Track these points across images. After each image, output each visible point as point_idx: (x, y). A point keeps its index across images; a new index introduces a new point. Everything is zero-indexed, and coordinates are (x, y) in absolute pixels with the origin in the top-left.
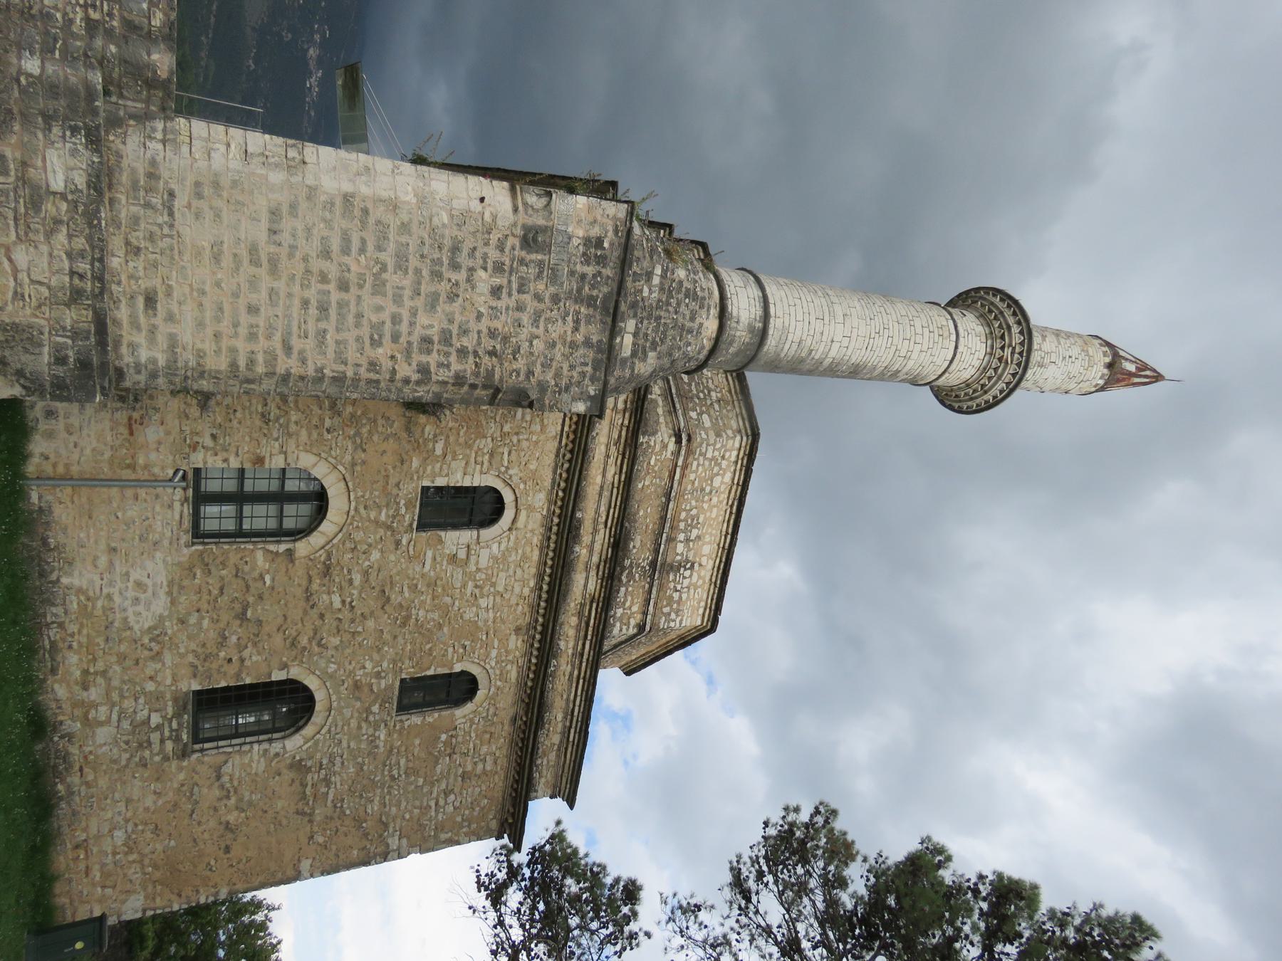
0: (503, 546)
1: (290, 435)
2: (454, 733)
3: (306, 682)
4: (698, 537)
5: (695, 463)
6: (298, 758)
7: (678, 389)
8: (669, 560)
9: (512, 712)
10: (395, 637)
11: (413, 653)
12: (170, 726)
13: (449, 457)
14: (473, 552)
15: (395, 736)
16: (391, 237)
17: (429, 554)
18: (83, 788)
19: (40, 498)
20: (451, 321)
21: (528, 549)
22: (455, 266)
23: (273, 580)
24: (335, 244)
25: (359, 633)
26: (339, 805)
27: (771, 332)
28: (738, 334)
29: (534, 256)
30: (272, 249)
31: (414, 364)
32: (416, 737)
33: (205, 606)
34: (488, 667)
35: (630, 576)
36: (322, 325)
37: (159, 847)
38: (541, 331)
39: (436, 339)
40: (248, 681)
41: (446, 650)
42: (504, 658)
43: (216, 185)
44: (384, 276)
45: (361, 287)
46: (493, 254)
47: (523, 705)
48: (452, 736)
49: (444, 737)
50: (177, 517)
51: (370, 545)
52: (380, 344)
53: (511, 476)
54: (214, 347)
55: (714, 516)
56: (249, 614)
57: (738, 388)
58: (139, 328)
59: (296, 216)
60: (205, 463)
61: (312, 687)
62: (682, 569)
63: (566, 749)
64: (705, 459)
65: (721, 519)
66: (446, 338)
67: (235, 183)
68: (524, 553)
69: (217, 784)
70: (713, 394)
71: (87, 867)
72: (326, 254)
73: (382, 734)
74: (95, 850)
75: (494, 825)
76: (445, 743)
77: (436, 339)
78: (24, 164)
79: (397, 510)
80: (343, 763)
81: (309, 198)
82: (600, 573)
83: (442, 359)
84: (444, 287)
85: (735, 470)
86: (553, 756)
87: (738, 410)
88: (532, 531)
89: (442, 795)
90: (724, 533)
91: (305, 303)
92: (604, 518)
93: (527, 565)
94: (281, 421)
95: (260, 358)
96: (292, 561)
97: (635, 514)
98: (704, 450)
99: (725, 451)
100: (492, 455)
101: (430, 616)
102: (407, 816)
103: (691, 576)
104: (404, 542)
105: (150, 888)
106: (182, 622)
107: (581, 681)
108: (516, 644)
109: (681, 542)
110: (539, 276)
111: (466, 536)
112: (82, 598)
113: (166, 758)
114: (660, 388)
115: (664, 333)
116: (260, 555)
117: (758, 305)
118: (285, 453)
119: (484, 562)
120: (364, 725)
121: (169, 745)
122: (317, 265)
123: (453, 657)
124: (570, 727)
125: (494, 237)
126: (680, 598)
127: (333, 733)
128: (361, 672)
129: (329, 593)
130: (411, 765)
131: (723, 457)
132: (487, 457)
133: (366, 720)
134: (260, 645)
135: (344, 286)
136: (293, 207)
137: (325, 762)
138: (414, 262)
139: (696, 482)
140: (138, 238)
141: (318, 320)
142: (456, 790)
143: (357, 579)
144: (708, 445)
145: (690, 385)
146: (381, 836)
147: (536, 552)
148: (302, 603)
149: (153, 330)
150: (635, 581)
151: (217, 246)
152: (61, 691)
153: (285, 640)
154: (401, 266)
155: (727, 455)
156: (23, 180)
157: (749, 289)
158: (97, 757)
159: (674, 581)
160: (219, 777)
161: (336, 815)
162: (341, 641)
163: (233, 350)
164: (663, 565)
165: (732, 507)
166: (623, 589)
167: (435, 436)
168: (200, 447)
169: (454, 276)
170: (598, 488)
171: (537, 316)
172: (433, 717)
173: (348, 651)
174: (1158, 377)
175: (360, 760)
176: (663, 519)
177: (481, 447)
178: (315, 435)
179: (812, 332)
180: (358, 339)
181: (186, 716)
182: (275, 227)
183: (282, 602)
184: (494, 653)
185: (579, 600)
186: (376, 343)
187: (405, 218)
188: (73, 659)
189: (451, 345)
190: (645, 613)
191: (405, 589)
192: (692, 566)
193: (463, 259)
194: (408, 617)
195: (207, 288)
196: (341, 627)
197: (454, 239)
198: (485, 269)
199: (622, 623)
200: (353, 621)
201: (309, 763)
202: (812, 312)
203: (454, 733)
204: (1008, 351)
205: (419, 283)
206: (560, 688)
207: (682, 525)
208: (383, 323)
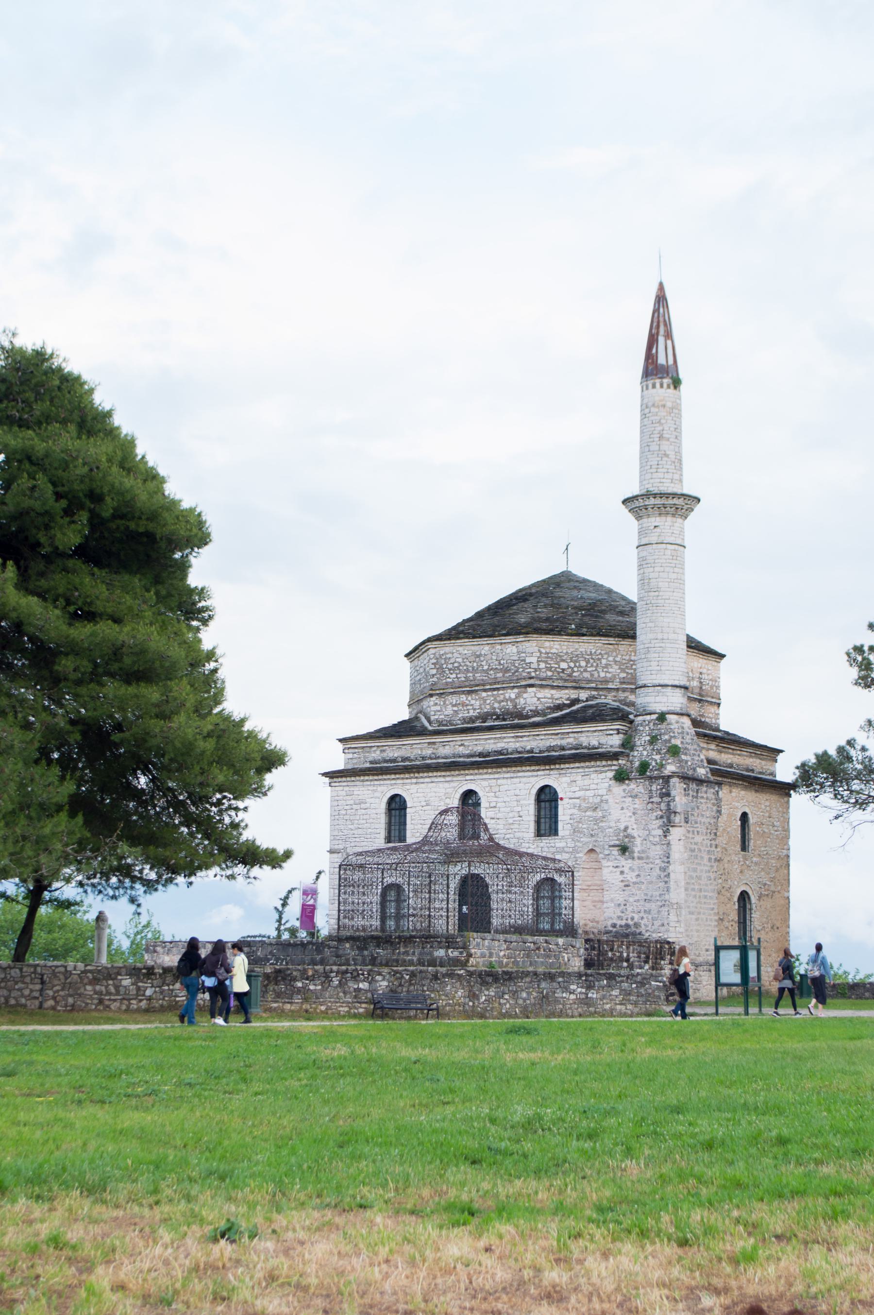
9: (753, 793)
24: (693, 893)
35: (702, 716)
73: (754, 859)
75: (786, 799)
86: (763, 763)
136: (689, 907)
140: (697, 953)
145: (627, 673)
151: (698, 931)
164: (700, 695)
171: (703, 815)
174: (661, 287)
184: (737, 804)
193: (693, 846)
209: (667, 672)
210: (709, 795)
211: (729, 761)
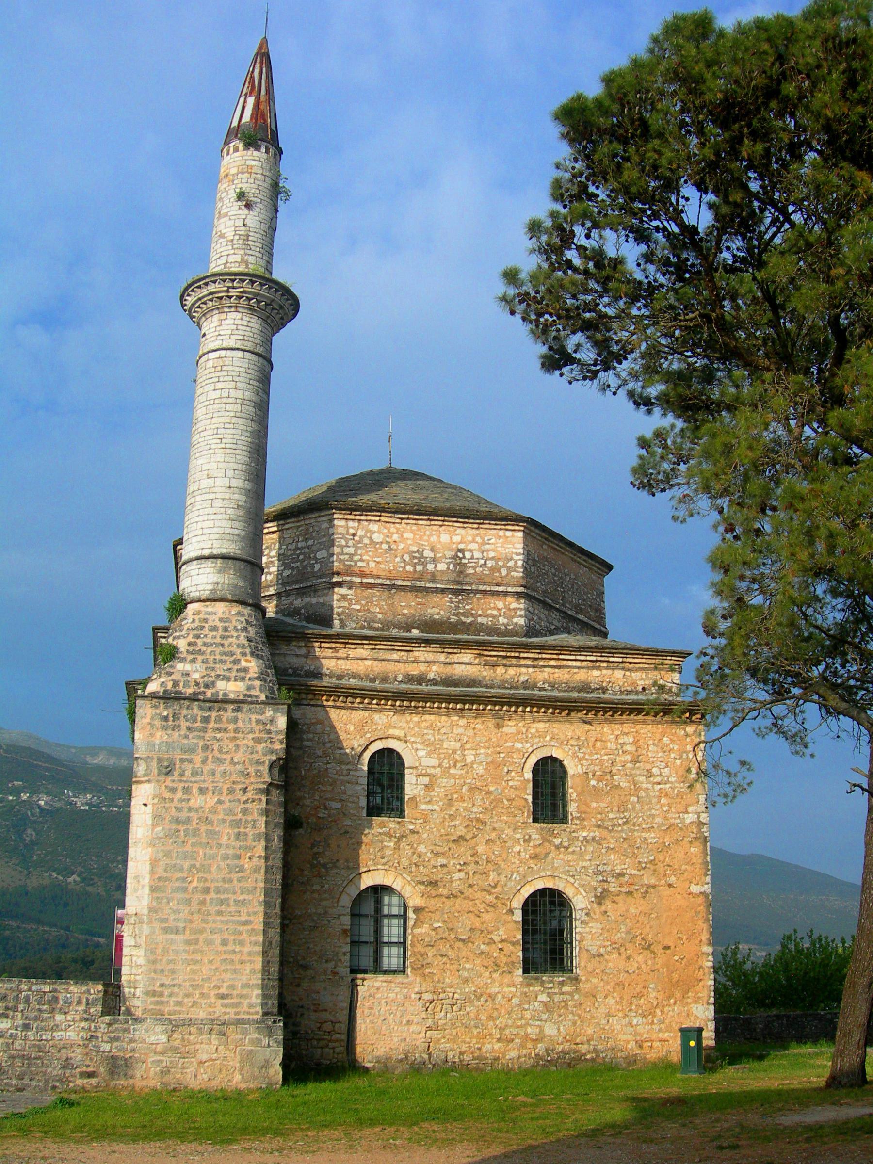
0: (419, 746)
1: (326, 913)
2: (590, 774)
3: (527, 895)
4: (432, 550)
5: (360, 564)
6: (593, 899)
7: (297, 582)
8: (453, 576)
10: (494, 829)
11: (509, 814)
12: (551, 988)
13: (344, 797)
14: (424, 771)
15: (586, 823)
16: (174, 862)
17: (423, 807)
18: (592, 1043)
19: (370, 1062)
20: (224, 821)
21: (424, 724)
22: (188, 820)
23: (438, 921)
24: (180, 895)
25: (488, 857)
26: (643, 865)
27: (224, 551)
28: (227, 582)
29: (177, 766)
30: (187, 932)
31: (254, 844)
32: (589, 807)
33: (455, 966)
34: (530, 750)
36: (232, 903)
37: (653, 994)
38: (228, 757)
39: (236, 830)
40: (519, 936)
41: (511, 787)
42: (524, 736)
43: (154, 962)
44: (198, 866)
45: (206, 880)
46: (179, 795)
47: (573, 714)
48: (593, 775)
49: (593, 782)
50: (384, 984)
51: (414, 853)
52: (243, 866)
53: (359, 746)
54: (248, 964)
55: (411, 536)
56: (463, 937)
57: (293, 520)
58: (240, 1003)
59: (167, 919)
60: (346, 967)
61: (531, 891)
62: (464, 561)
63: (630, 663)
64: (356, 554)
65: (414, 528)
66: (237, 823)
67: (153, 952)
68: (427, 728)
69: (606, 957)
70: (300, 545)
71: (660, 1041)
72: (188, 902)
74: (645, 1036)
76: (599, 781)
77: (236, 830)
78: (155, 1053)
79: (385, 834)
80: (605, 864)
81: (156, 912)
82: (455, 651)
83: (250, 825)
84: (203, 828)
85: (367, 521)
86: (636, 675)
87: (312, 521)
88: (407, 722)
89: (652, 779)
90: (428, 523)
91: (220, 913)
92: (403, 653)
93: (439, 724)
94: (315, 918)
95: (253, 939)
96: (423, 909)
97: (408, 618)
98: (347, 557)
99: (348, 533)
100: (341, 763)
101: (478, 802)
102: (665, 808)
103: (471, 551)
104: (412, 827)
105: (689, 1000)
106: (466, 981)
107: (561, 657)
108: (511, 727)
109: (436, 566)
110: (190, 761)
111: (409, 778)
112: (443, 1041)
113: (577, 990)
114: (296, 599)
115: (225, 654)
116: (417, 931)
117: (203, 566)
118: (339, 916)
119: (434, 762)
120: (570, 850)
121: (566, 989)
122: (195, 907)
123: (518, 780)
124: (608, 661)
125: (168, 795)
126: (492, 558)
127: (574, 873)
128: (523, 854)
129: (452, 882)
130: (616, 809)
131: (354, 535)
132: (343, 767)
133: (567, 848)
134: (490, 929)
135: (207, 890)
137: (601, 878)
138: (188, 848)
139: (377, 560)
141: (228, 905)
142: (649, 767)
143: (441, 861)
144: (342, 554)
145: (293, 568)
146: (681, 829)
147: (427, 717)
148: (458, 901)
149: (241, 996)
150: (472, 609)
152: (513, 1054)
153: (488, 912)
154: (192, 856)
155: (352, 531)
156: (162, 1053)
157: (193, 573)
158: (567, 1034)
159: (474, 567)
160: (600, 955)
161: (653, 868)
162: (493, 871)
163: (250, 954)
165: (402, 519)
166: (479, 620)
167: (326, 809)
168: (335, 970)
169: (195, 821)
170: (376, 663)
172: (572, 793)
173: (503, 865)
175: (604, 851)
176: (414, 589)
177: (335, 772)
178: (326, 896)
179: (223, 510)
180: (239, 881)
181: (544, 978)
182: (175, 931)
183: (456, 914)
184: (518, 745)
185: (482, 669)
186: (241, 870)
187: (161, 854)
188: (487, 1047)
189: (241, 819)
190: (506, 594)
191: (452, 824)
192: (460, 550)
193: (184, 815)
194: (478, 820)
195: (214, 967)
196: (481, 871)
197: (171, 822)
198: (189, 800)
199: (513, 617)
200: (477, 863)
201: (600, 890)
202: (207, 511)
203: (590, 774)
204: (233, 292)
205: (201, 843)
206: (566, 676)
207: (419, 568)
208: (228, 865)
209: (194, 540)
210: (240, 724)
211: (523, 679)
